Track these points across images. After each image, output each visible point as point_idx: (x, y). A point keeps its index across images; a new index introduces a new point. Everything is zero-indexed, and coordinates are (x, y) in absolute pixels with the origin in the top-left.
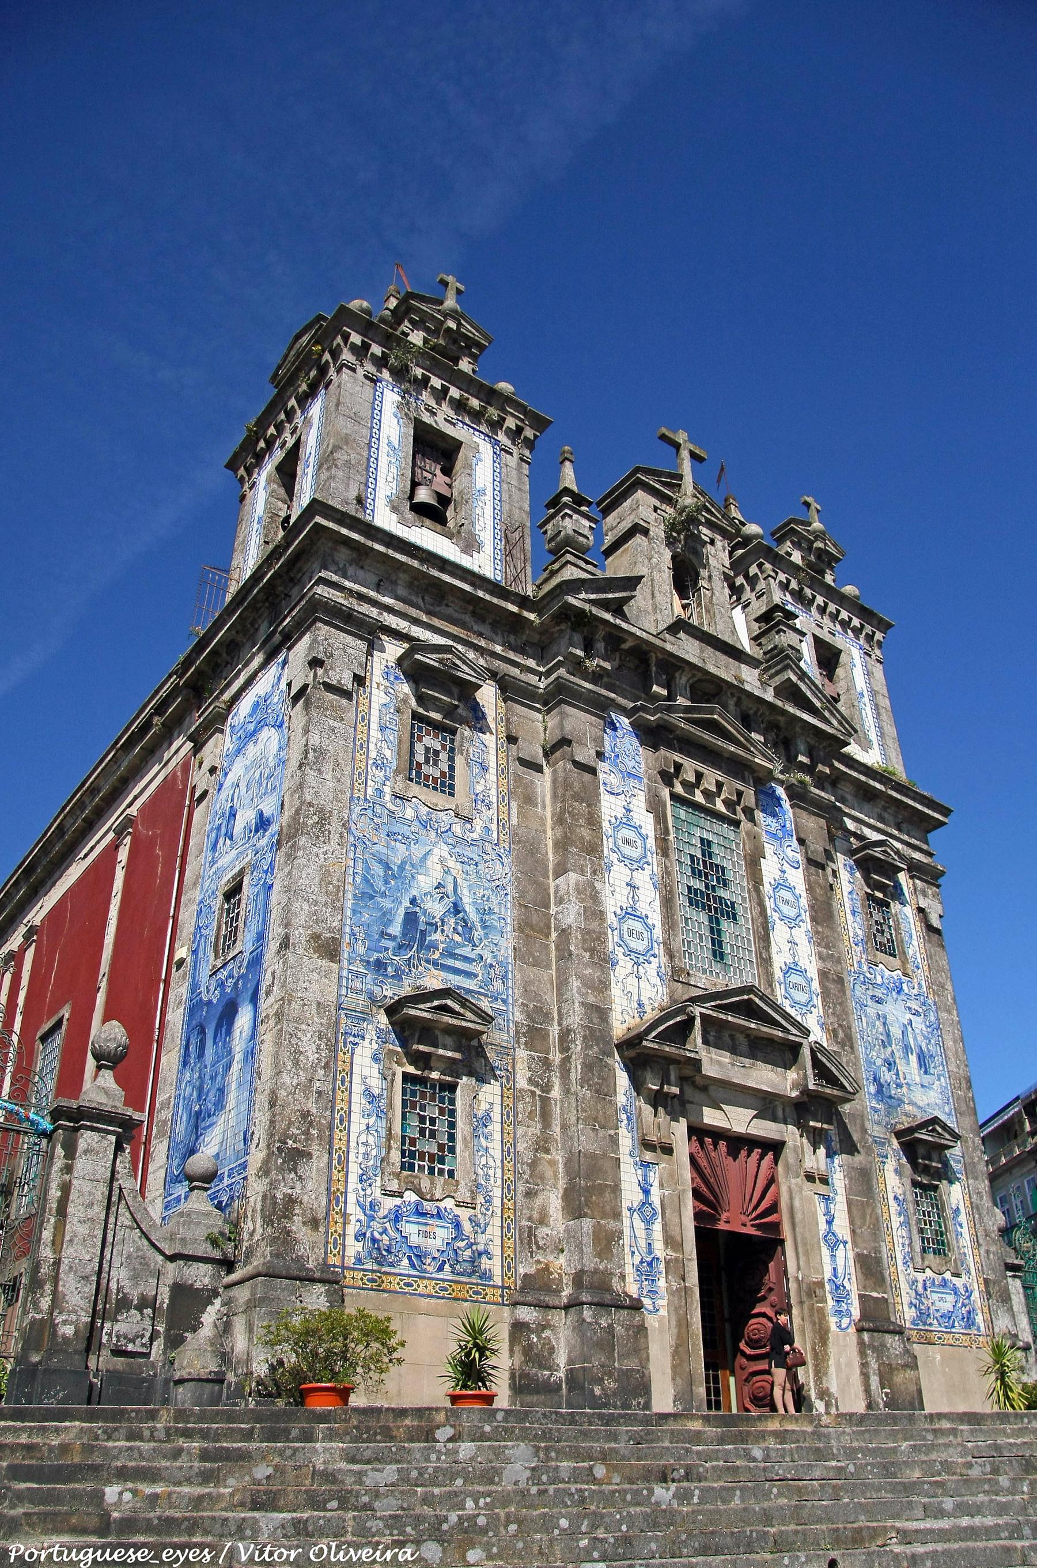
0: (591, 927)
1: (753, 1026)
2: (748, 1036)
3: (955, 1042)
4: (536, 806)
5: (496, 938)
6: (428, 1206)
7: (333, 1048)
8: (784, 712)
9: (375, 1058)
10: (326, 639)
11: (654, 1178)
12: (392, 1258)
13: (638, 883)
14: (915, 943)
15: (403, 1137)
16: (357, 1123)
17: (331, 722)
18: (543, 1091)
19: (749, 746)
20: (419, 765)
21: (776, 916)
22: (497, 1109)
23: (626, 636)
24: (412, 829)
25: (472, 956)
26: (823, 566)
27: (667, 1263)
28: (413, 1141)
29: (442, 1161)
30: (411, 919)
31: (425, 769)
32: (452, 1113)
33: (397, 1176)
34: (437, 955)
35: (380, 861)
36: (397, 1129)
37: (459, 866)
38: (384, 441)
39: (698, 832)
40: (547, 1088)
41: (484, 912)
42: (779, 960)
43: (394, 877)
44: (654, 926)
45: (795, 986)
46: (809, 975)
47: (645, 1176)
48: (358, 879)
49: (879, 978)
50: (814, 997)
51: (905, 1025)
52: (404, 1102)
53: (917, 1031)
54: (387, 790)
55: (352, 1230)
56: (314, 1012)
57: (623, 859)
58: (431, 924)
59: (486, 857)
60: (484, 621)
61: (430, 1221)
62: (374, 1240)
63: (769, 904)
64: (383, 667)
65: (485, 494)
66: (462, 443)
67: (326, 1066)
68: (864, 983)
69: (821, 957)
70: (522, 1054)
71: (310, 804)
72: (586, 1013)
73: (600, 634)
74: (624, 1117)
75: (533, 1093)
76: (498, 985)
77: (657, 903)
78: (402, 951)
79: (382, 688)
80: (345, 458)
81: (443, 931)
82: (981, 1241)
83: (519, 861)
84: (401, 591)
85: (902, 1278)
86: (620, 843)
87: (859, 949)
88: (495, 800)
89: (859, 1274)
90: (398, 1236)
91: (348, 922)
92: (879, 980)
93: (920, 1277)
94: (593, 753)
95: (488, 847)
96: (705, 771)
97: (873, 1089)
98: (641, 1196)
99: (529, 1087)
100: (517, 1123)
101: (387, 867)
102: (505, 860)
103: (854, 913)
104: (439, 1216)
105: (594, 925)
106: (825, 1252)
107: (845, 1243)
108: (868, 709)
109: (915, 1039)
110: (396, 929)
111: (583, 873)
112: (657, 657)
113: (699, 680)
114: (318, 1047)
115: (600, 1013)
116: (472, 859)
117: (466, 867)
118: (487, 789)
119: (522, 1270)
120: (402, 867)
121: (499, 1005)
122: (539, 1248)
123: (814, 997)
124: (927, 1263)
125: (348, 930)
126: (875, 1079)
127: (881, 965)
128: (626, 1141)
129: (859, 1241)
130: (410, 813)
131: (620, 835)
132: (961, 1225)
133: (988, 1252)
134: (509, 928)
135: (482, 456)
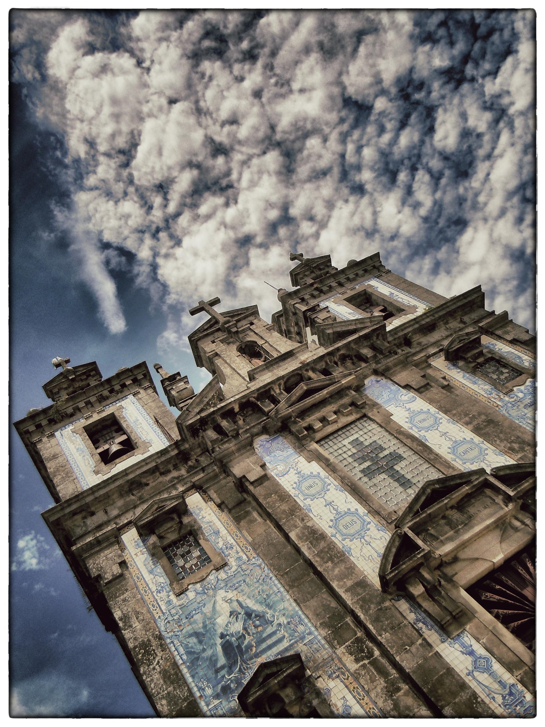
0: (321, 547)
1: (446, 501)
2: (452, 508)
4: (256, 520)
5: (281, 606)
8: (338, 349)
10: (94, 564)
13: (331, 500)
17: (122, 597)
18: (368, 658)
19: (334, 381)
20: (183, 567)
21: (423, 433)
22: (349, 697)
23: (230, 407)
24: (198, 601)
25: (274, 629)
26: (327, 270)
30: (227, 647)
31: (187, 566)
34: (254, 649)
35: (190, 636)
37: (235, 592)
39: (346, 442)
40: (370, 654)
44: (357, 510)
46: (468, 439)
48: (185, 657)
57: (313, 497)
58: (240, 637)
59: (246, 573)
60: (169, 471)
63: (414, 432)
64: (134, 544)
65: (138, 420)
66: (113, 413)
69: (467, 424)
70: (341, 650)
71: (135, 647)
72: (352, 594)
73: (219, 419)
74: (420, 625)
75: (364, 666)
76: (301, 628)
78: (233, 668)
80: (60, 477)
81: (249, 634)
83: (264, 556)
84: (120, 503)
86: (306, 491)
87: (494, 395)
88: (232, 541)
91: (193, 685)
92: (521, 395)
94: (259, 469)
95: (244, 567)
96: (324, 414)
99: (359, 665)
100: (368, 692)
101: (196, 634)
103: (475, 383)
110: (222, 661)
111: (296, 527)
112: (254, 397)
113: (285, 383)
115: (363, 584)
116: (240, 581)
117: (241, 588)
120: (205, 626)
127: (515, 389)
131: (303, 488)
134: (285, 593)
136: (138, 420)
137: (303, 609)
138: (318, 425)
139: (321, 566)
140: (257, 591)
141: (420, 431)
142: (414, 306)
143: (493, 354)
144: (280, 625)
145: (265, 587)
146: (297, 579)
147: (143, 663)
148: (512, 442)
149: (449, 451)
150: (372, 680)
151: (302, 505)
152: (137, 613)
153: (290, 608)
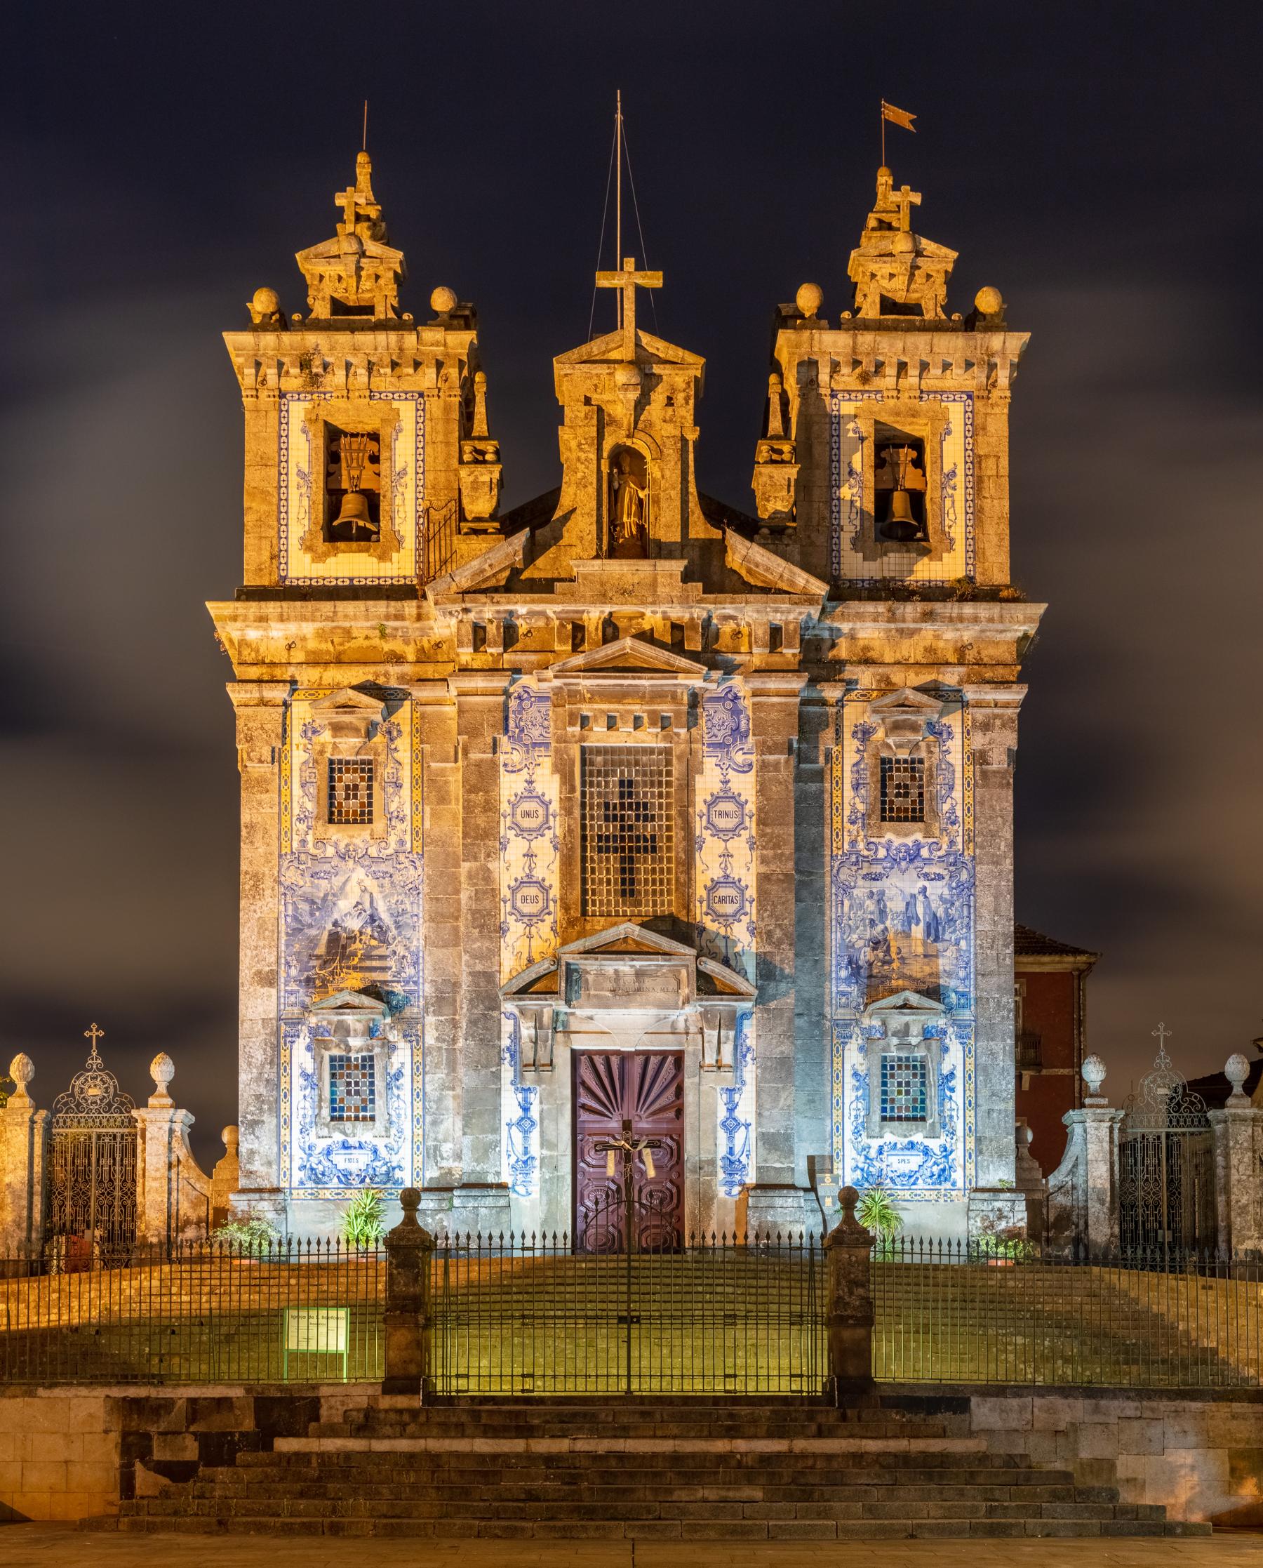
3: (996, 898)
4: (450, 803)
5: (407, 933)
6: (352, 1141)
7: (276, 1048)
9: (309, 1048)
11: (534, 1099)
12: (326, 1179)
13: (535, 851)
14: (957, 794)
15: (333, 1101)
16: (297, 1095)
17: (258, 796)
20: (340, 804)
27: (542, 1160)
28: (342, 1100)
29: (365, 1109)
30: (334, 938)
32: (372, 1075)
33: (327, 1125)
35: (306, 900)
36: (327, 1094)
37: (375, 882)
38: (293, 471)
40: (454, 1041)
41: (397, 915)
42: (702, 878)
43: (318, 909)
45: (722, 900)
46: (743, 884)
47: (525, 1099)
48: (289, 919)
49: (882, 853)
50: (747, 904)
51: (913, 896)
52: (333, 1076)
53: (932, 898)
54: (310, 838)
55: (296, 1164)
56: (260, 1026)
61: (353, 1151)
62: (312, 1169)
63: (699, 825)
67: (271, 1063)
68: (856, 863)
69: (764, 860)
71: (246, 873)
74: (507, 1055)
75: (440, 1048)
77: (557, 863)
79: (301, 747)
82: (980, 1102)
85: (848, 1146)
88: (407, 811)
89: (761, 1150)
90: (329, 1164)
93: (875, 1144)
95: (402, 857)
97: (843, 973)
98: (520, 1113)
100: (425, 1073)
101: (313, 902)
102: (418, 864)
103: (856, 787)
104: (361, 1147)
105: (487, 904)
106: (722, 1135)
107: (747, 1126)
108: (959, 495)
109: (927, 906)
110: (321, 950)
114: (265, 1050)
115: (489, 977)
118: (402, 804)
119: (428, 1175)
120: (324, 899)
121: (412, 987)
122: (442, 1158)
123: (747, 904)
124: (887, 1129)
125: (283, 961)
126: (850, 962)
127: (889, 836)
128: (507, 1072)
129: (764, 1121)
130: (330, 851)
131: (519, 811)
132: (952, 1090)
133: (989, 1112)
134: (421, 921)
135: (403, 424)
136: (405, 474)
137: (427, 952)
138: (599, 729)
139: (467, 927)
140: (396, 898)
141: (707, 828)
142: (952, 541)
143: (931, 752)
144: (395, 953)
145: (406, 900)
146: (442, 915)
147: (246, 896)
148: (780, 926)
149: (709, 884)
150: (437, 1066)
151: (502, 834)
152: (266, 831)
153: (415, 943)
